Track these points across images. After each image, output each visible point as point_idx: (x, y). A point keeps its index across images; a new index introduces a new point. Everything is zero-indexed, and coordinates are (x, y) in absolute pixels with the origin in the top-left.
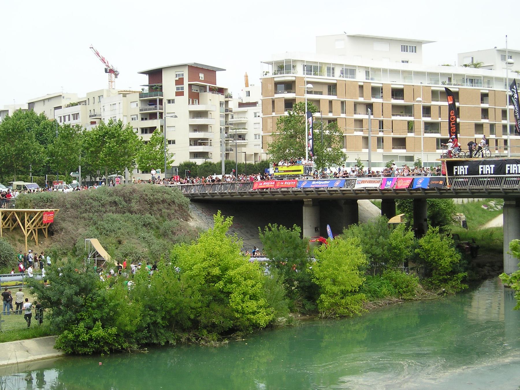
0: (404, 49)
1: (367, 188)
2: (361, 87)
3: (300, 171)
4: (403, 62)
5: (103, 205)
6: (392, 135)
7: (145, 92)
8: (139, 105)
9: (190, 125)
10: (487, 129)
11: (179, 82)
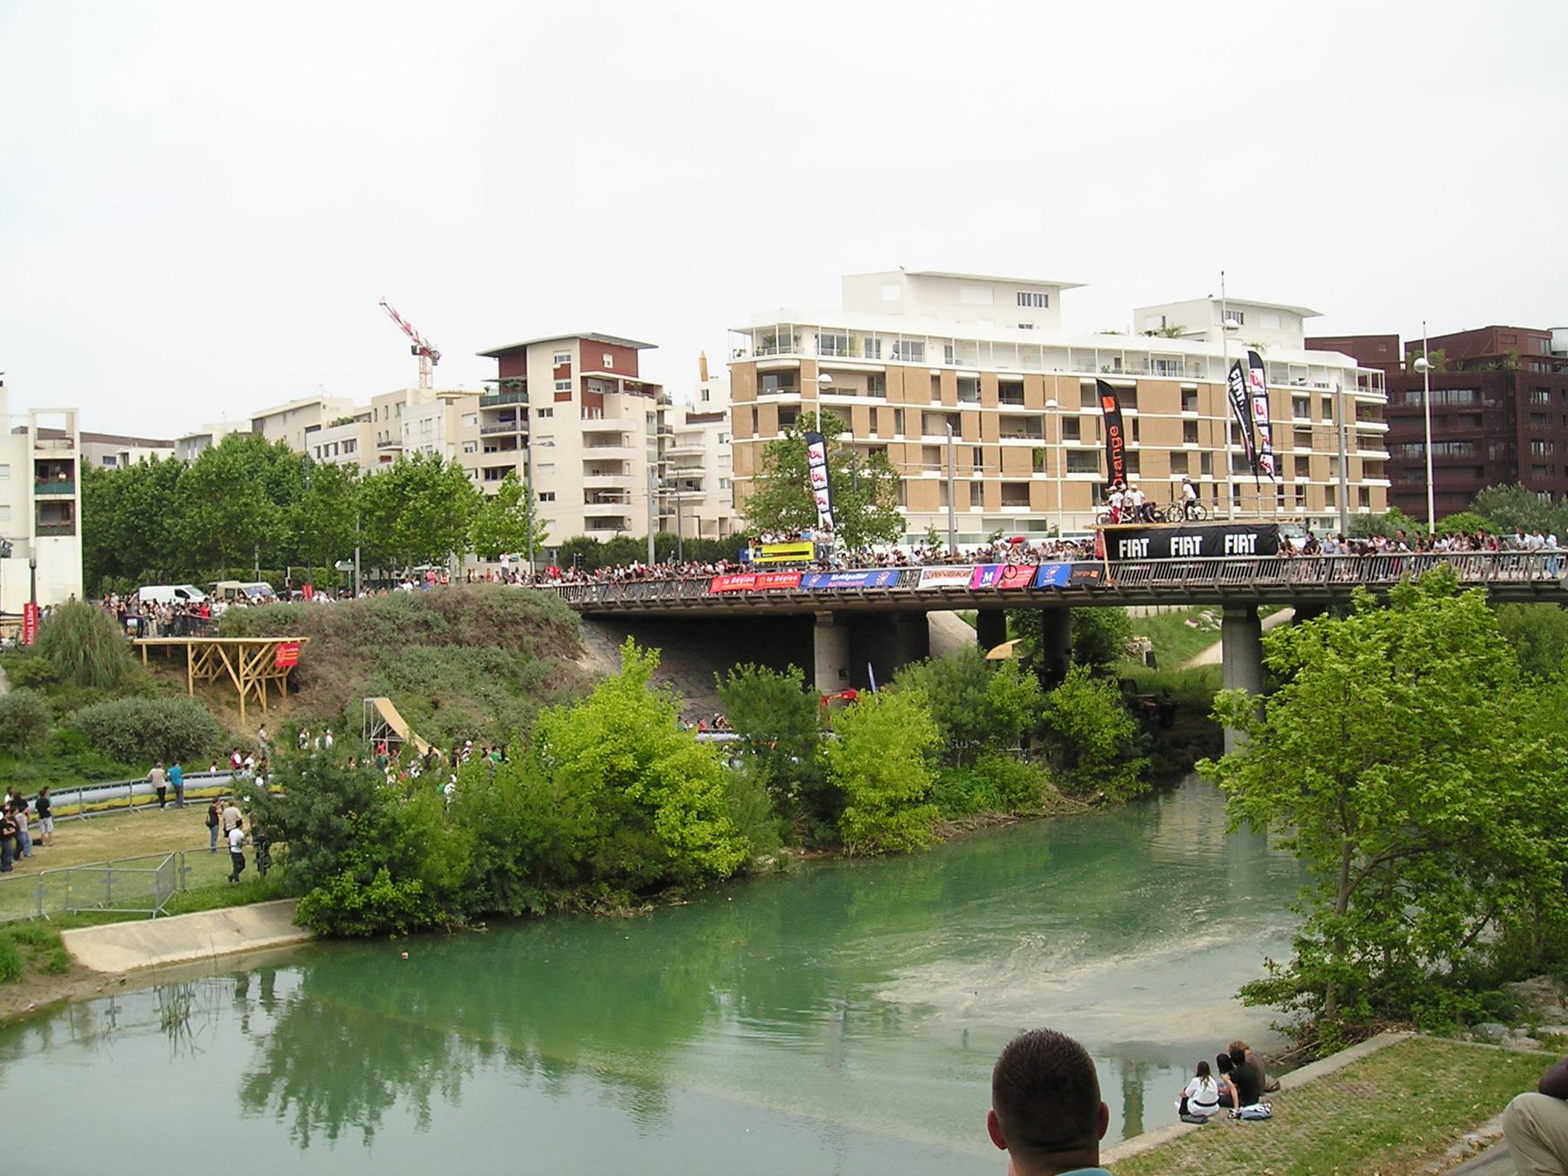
0: (1024, 300)
1: (772, 592)
2: (936, 379)
3: (807, 553)
4: (1021, 326)
5: (401, 629)
6: (1002, 478)
8: (480, 421)
9: (585, 461)
10: (1194, 463)
11: (563, 372)
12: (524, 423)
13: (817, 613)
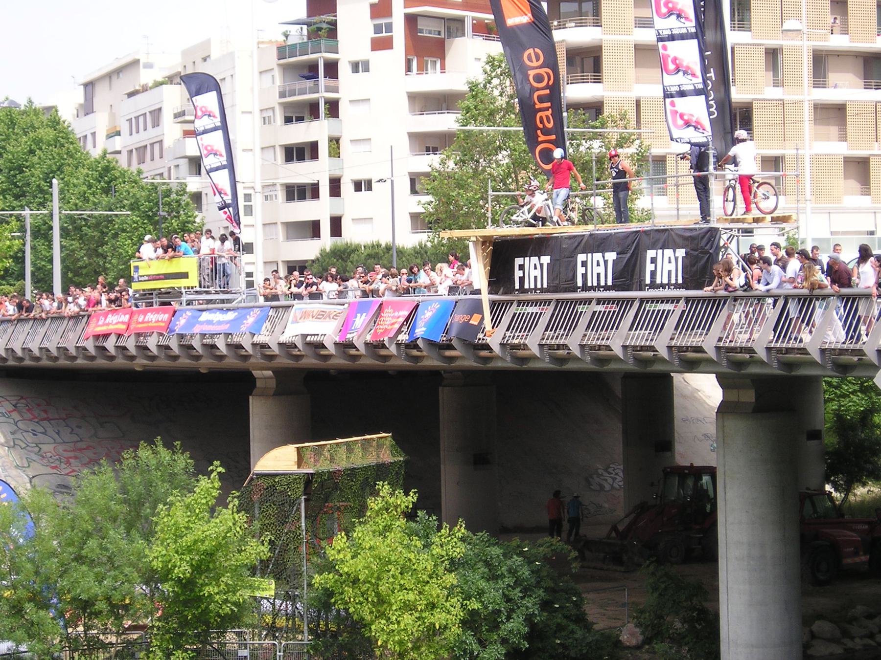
3: (185, 275)
7: (291, 41)
8: (278, 81)
12: (331, 82)
13: (256, 373)
